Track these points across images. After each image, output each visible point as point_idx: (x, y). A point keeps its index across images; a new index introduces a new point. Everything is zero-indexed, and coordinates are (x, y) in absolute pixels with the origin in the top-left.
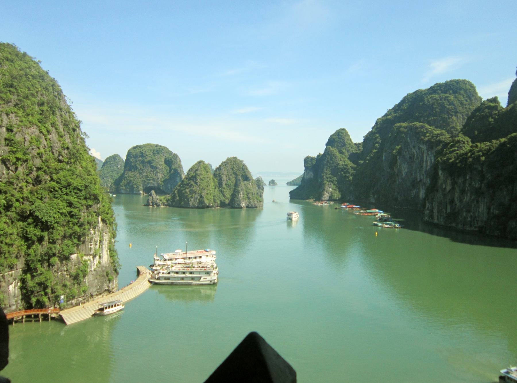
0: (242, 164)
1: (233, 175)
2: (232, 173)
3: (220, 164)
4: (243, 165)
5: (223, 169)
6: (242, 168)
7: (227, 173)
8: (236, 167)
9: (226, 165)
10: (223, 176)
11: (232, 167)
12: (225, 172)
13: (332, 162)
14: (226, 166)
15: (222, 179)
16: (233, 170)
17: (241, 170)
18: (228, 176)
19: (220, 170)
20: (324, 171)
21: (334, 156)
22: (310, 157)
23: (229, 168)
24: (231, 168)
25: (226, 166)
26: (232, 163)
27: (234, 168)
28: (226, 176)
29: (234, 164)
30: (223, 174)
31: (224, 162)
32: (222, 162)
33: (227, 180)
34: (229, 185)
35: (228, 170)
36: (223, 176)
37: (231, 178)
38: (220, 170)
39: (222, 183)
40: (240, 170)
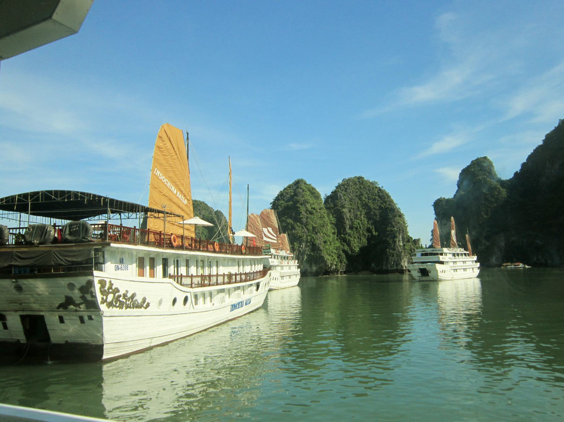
0: (376, 187)
1: (361, 209)
2: (359, 205)
3: (334, 189)
4: (380, 190)
5: (343, 198)
6: (379, 196)
7: (351, 204)
8: (367, 193)
9: (346, 189)
10: (344, 210)
11: (358, 194)
12: (346, 202)
13: (493, 200)
14: (346, 191)
15: (345, 216)
16: (360, 199)
17: (377, 197)
18: (352, 211)
19: (337, 199)
20: (483, 216)
21: (496, 189)
22: (444, 198)
23: (352, 195)
24: (357, 196)
25: (346, 191)
26: (358, 187)
27: (362, 195)
28: (350, 211)
29: (360, 187)
30: (343, 207)
31: (343, 185)
32: (337, 185)
33: (351, 219)
34: (357, 228)
35: (351, 200)
36: (344, 210)
37: (359, 216)
38: (337, 199)
39: (346, 223)
40: (375, 199)
